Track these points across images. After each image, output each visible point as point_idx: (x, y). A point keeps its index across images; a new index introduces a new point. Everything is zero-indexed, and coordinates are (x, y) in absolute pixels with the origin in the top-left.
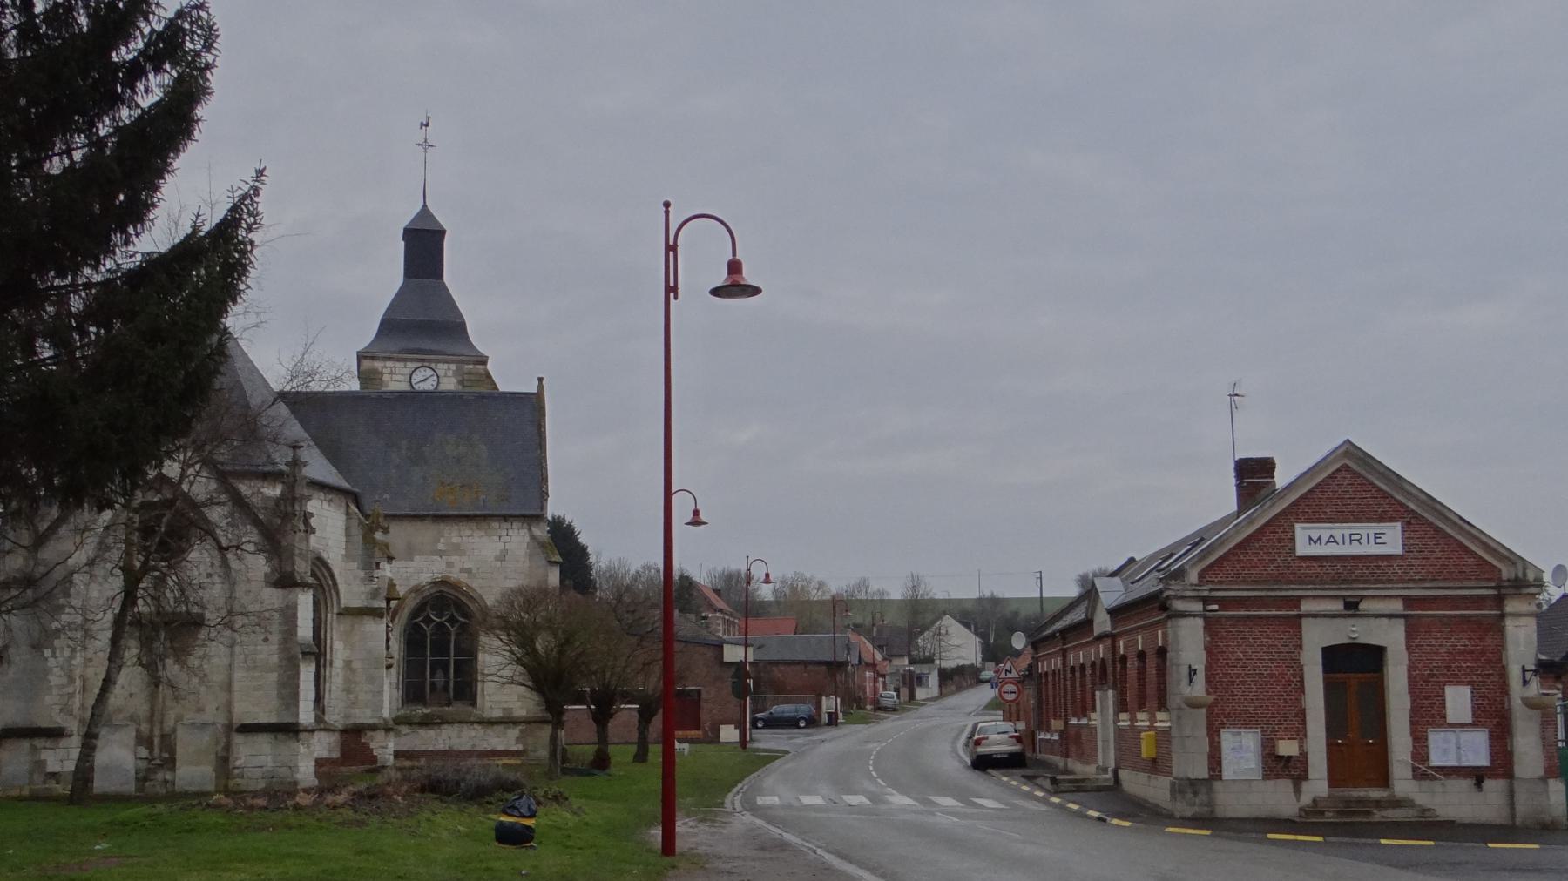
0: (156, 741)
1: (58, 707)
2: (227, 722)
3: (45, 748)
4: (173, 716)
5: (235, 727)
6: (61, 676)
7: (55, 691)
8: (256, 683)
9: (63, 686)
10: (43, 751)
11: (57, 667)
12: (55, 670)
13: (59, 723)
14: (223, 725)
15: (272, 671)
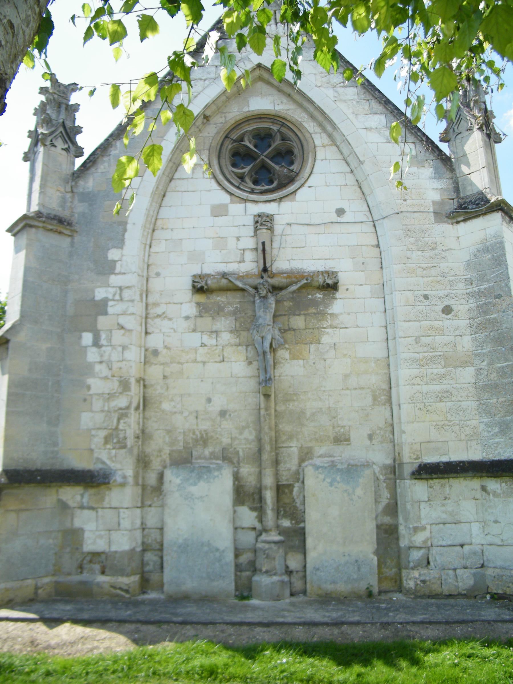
0: (269, 496)
1: (103, 434)
2: (389, 461)
3: (82, 507)
4: (295, 450)
5: (408, 470)
6: (106, 378)
7: (97, 405)
8: (438, 388)
9: (111, 396)
10: (78, 512)
11: (101, 362)
12: (98, 368)
13: (104, 463)
14: (385, 467)
15: (464, 364)
